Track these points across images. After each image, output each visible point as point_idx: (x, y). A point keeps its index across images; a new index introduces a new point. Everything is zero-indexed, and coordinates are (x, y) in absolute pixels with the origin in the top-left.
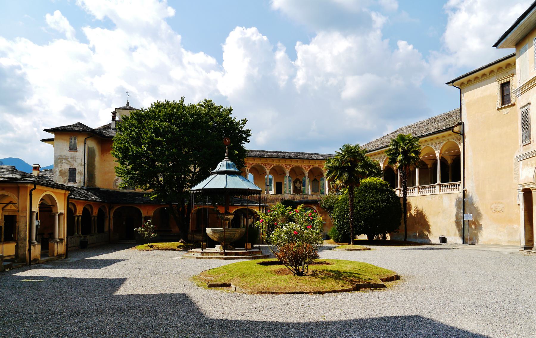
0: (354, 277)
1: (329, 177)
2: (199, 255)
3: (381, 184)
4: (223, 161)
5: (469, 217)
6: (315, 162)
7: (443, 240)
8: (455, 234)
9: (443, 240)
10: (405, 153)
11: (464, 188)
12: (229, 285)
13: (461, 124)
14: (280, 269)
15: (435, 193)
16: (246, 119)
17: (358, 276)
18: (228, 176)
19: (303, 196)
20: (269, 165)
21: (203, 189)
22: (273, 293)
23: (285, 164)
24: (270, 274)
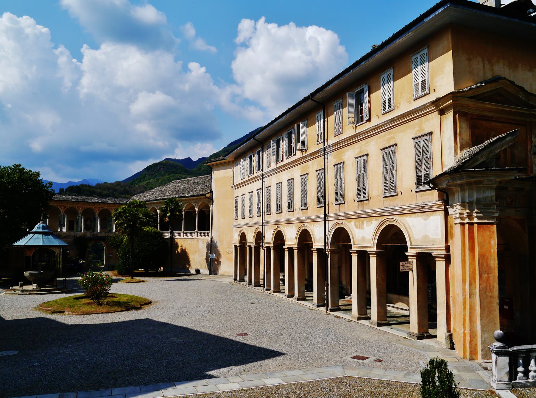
0: (127, 304)
1: (116, 222)
2: (20, 292)
3: (155, 232)
4: (40, 224)
5: (213, 256)
6: (105, 205)
7: (198, 271)
8: (205, 267)
9: (198, 271)
10: (172, 211)
11: (211, 236)
12: (64, 312)
13: (212, 192)
14: (89, 302)
15: (194, 238)
16: (52, 182)
17: (129, 303)
18: (43, 235)
19: (93, 233)
20: (63, 207)
21: (24, 246)
22: (88, 314)
23: (78, 206)
24: (85, 305)
